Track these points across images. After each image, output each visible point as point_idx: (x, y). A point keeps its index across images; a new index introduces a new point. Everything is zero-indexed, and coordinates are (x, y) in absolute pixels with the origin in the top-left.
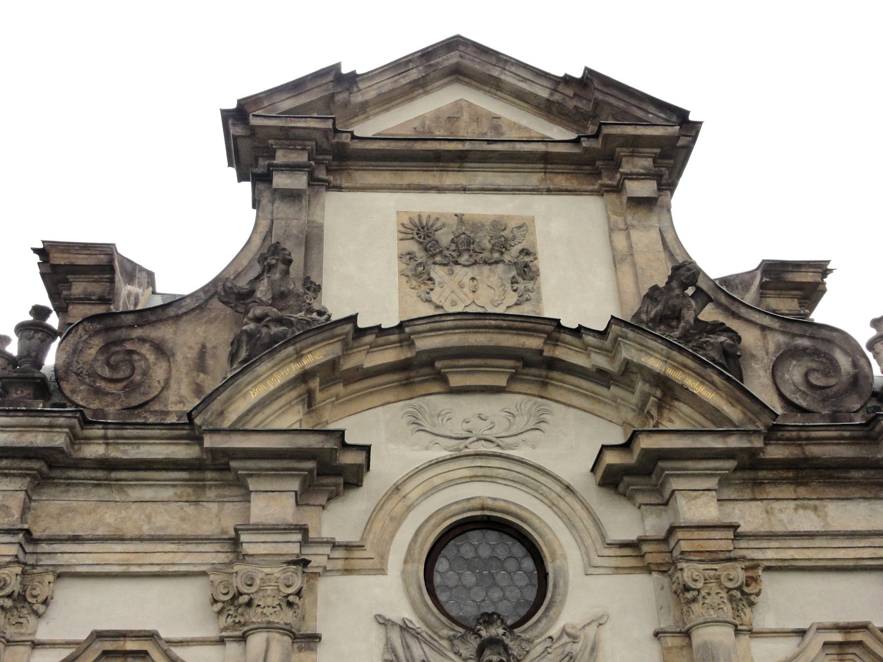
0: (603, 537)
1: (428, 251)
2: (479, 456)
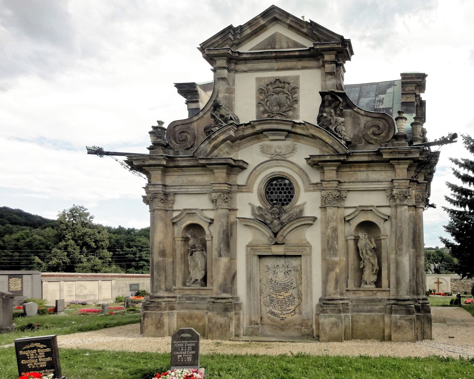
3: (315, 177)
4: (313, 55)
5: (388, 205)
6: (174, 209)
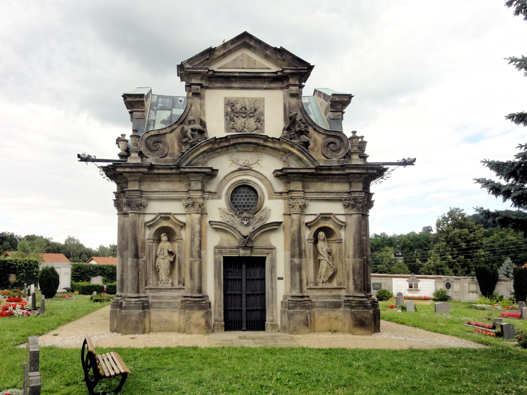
0: (273, 190)
1: (233, 112)
2: (244, 169)
3: (279, 186)
4: (276, 80)
5: (344, 213)
6: (146, 212)
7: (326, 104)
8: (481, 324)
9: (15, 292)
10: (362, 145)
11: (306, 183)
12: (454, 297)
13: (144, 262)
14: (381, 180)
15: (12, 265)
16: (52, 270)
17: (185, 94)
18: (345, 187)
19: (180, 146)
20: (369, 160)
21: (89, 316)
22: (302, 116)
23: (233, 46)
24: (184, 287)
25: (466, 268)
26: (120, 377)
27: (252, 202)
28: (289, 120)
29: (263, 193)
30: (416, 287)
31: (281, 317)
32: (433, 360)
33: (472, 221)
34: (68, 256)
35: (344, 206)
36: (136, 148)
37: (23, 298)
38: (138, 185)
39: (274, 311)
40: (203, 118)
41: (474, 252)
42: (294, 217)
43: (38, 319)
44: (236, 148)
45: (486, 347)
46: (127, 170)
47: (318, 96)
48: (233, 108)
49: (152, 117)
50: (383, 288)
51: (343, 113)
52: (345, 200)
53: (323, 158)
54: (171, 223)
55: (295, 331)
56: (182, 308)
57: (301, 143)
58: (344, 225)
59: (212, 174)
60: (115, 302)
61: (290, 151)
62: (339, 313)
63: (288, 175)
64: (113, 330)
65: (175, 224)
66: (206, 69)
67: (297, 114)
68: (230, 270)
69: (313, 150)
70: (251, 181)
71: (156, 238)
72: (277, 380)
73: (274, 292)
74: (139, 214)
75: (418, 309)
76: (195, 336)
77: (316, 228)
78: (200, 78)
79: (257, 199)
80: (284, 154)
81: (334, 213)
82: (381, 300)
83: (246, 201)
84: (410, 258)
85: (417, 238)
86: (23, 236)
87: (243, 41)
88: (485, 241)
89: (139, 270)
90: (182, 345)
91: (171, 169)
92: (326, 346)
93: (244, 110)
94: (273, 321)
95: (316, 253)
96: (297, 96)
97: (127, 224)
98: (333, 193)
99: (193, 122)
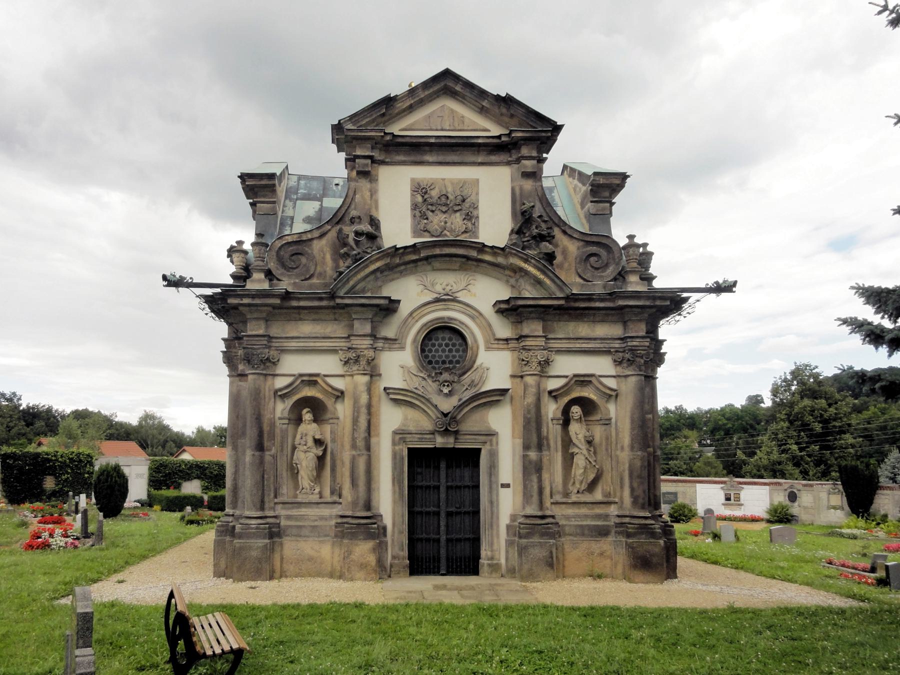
0: (494, 335)
1: (425, 203)
2: (446, 299)
3: (503, 329)
4: (498, 149)
5: (614, 374)
6: (278, 372)
7: (584, 188)
8: (851, 563)
9: (53, 506)
10: (645, 258)
11: (549, 323)
12: (804, 517)
13: (273, 456)
14: (678, 318)
15: (49, 460)
16: (117, 469)
17: (344, 173)
18: (616, 330)
19: (335, 261)
20: (657, 284)
21: (178, 548)
22: (542, 210)
23: (427, 93)
24: (341, 500)
25: (822, 466)
26: (232, 657)
27: (457, 354)
28: (520, 217)
29: (476, 341)
30: (738, 498)
31: (507, 552)
32: (769, 628)
33: (832, 386)
34: (143, 445)
35: (615, 361)
36: (261, 263)
37: (66, 518)
38: (263, 326)
39: (495, 541)
40: (374, 214)
41: (836, 439)
42: (530, 380)
43: (93, 553)
44: (430, 264)
45: (861, 604)
46: (246, 301)
47: (570, 176)
48: (426, 197)
49: (289, 212)
50: (680, 500)
51: (612, 204)
52: (617, 351)
53: (579, 280)
54: (319, 392)
55: (530, 576)
56: (336, 536)
57: (541, 256)
58: (614, 394)
59: (390, 307)
60: (222, 526)
61: (521, 269)
62: (607, 545)
63: (520, 309)
64: (219, 574)
65: (325, 392)
66: (381, 131)
67: (533, 206)
68: (419, 470)
69: (561, 266)
70: (455, 320)
71: (293, 416)
72: (501, 662)
73: (495, 509)
74: (266, 375)
75: (741, 538)
76: (358, 584)
77: (566, 399)
78: (370, 146)
79: (465, 351)
80: (512, 274)
81: (598, 373)
82: (678, 521)
83: (447, 353)
84: (726, 450)
85: (738, 416)
86: (68, 411)
87: (442, 84)
88: (854, 420)
89: (264, 471)
90: (337, 600)
91: (321, 299)
92: (584, 602)
93: (443, 199)
94: (492, 558)
95: (567, 442)
96: (534, 175)
97: (245, 393)
98: (595, 339)
99: (357, 220)
